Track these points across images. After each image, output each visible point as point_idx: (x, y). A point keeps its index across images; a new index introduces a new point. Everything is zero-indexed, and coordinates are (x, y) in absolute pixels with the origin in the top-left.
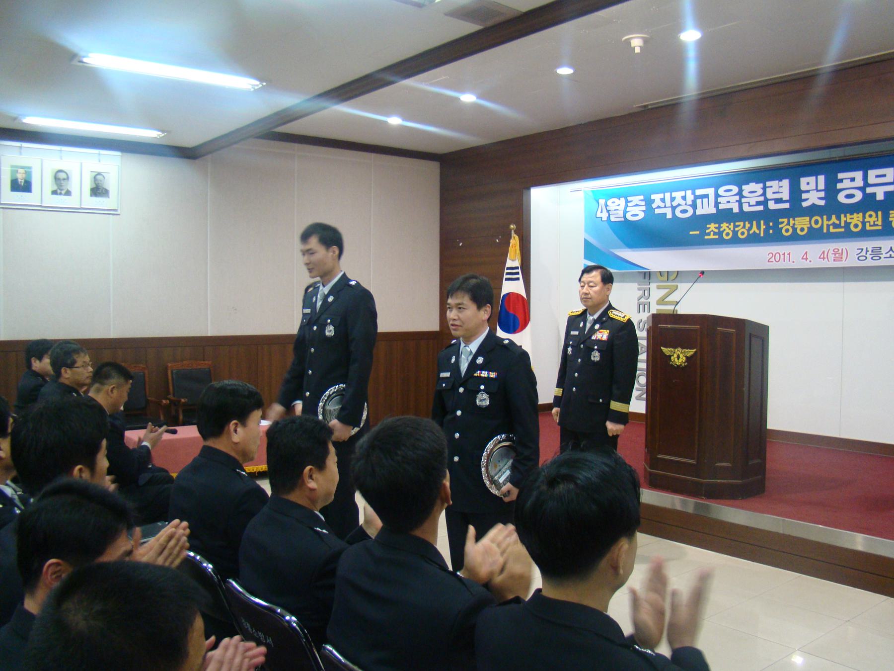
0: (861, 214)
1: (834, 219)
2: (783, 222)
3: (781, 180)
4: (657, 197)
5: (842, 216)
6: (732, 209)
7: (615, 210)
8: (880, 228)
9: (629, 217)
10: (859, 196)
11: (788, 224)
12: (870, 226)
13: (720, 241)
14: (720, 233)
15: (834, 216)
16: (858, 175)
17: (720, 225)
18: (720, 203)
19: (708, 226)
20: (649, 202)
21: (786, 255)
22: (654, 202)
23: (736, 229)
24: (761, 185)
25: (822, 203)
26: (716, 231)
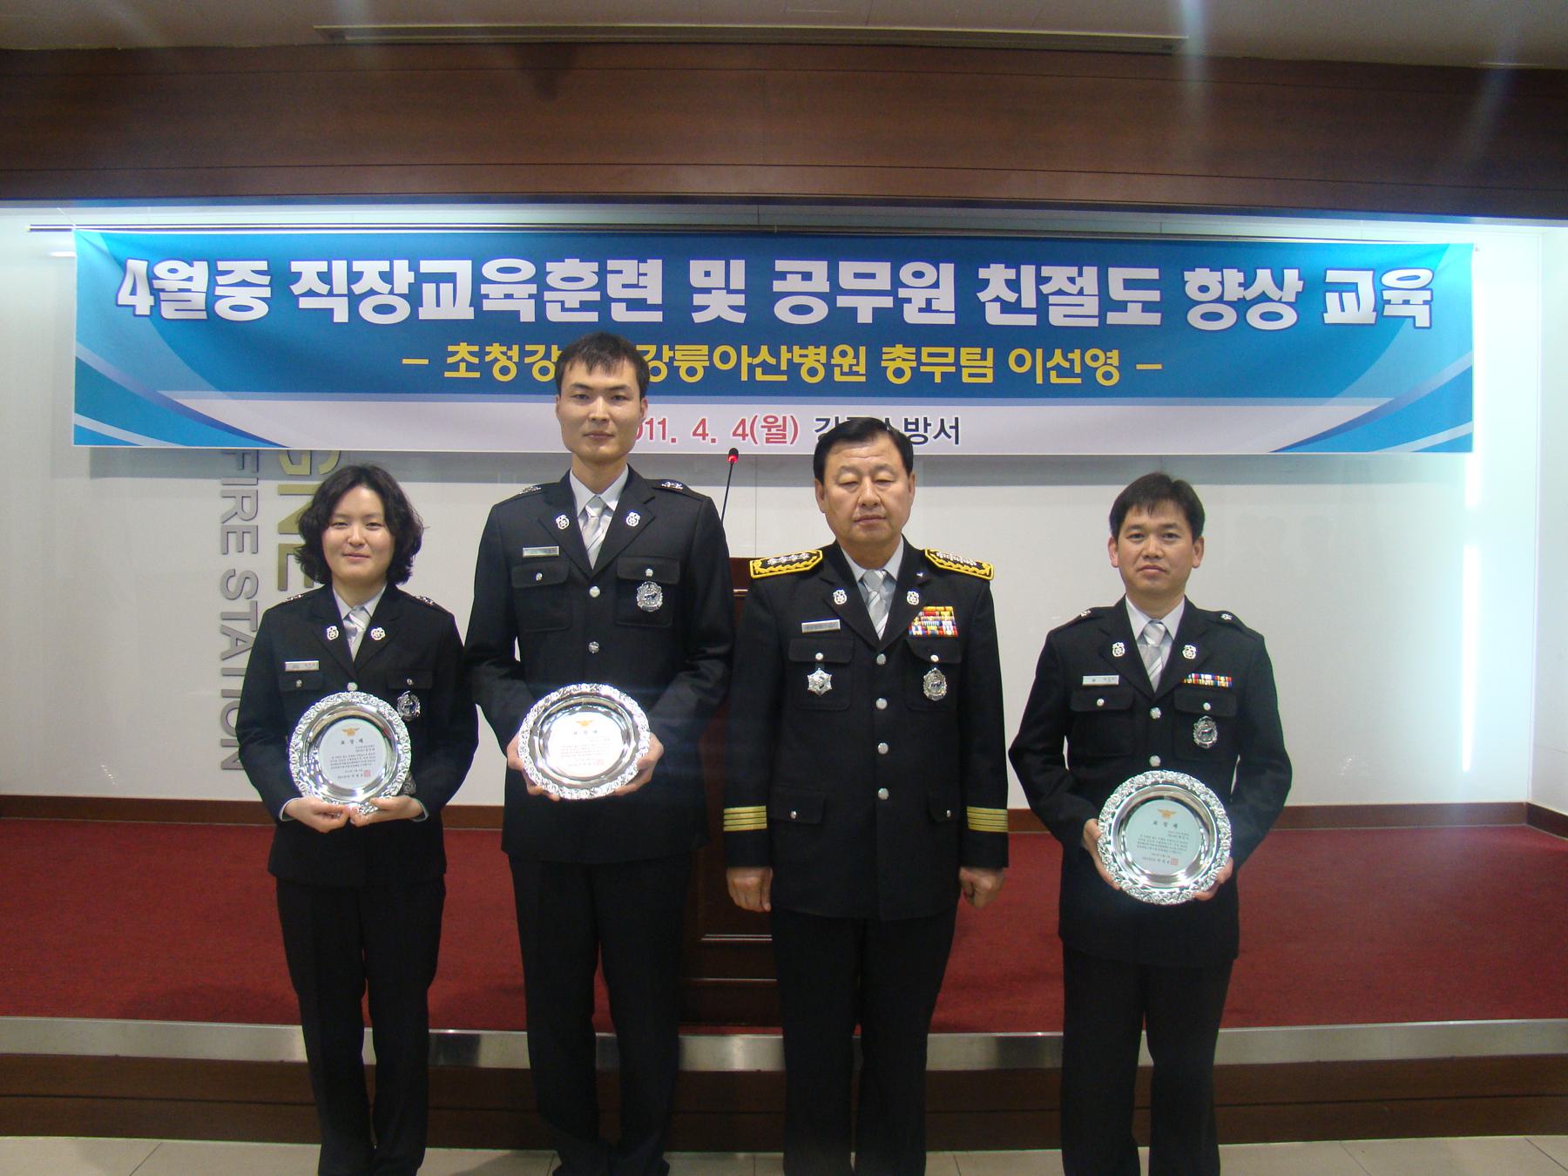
0: (823, 350)
1: (764, 354)
3: (642, 260)
4: (309, 270)
5: (784, 348)
6: (518, 313)
8: (863, 379)
9: (222, 308)
10: (820, 311)
11: (658, 356)
12: (843, 374)
13: (484, 385)
14: (485, 368)
15: (764, 349)
16: (819, 268)
18: (487, 296)
19: (451, 348)
20: (281, 279)
21: (655, 423)
23: (528, 360)
24: (595, 266)
25: (740, 318)
26: (476, 360)
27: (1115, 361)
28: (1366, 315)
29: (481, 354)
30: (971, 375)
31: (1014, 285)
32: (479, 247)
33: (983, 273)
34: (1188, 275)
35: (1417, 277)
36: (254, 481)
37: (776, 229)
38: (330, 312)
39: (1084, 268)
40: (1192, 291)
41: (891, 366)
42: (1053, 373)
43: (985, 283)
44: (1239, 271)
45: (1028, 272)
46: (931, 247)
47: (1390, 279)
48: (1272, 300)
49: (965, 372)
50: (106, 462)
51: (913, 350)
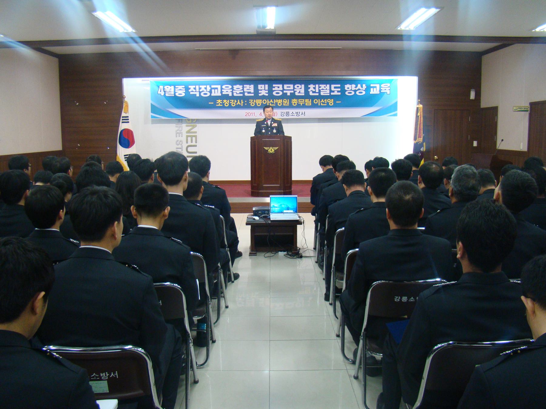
0: (281, 100)
1: (271, 101)
4: (192, 87)
5: (275, 100)
8: (288, 105)
9: (177, 94)
10: (281, 93)
11: (253, 102)
13: (223, 107)
14: (223, 104)
15: (271, 100)
16: (281, 86)
18: (223, 92)
19: (217, 101)
20: (187, 89)
23: (230, 103)
24: (242, 86)
25: (267, 95)
26: (222, 103)
29: (222, 102)
32: (222, 83)
33: (309, 86)
34: (345, 86)
35: (387, 85)
36: (181, 124)
40: (346, 89)
41: (293, 103)
42: (322, 103)
43: (309, 88)
44: (355, 85)
45: (317, 86)
46: (300, 82)
47: (382, 86)
49: (306, 103)
50: (155, 121)
51: (297, 100)
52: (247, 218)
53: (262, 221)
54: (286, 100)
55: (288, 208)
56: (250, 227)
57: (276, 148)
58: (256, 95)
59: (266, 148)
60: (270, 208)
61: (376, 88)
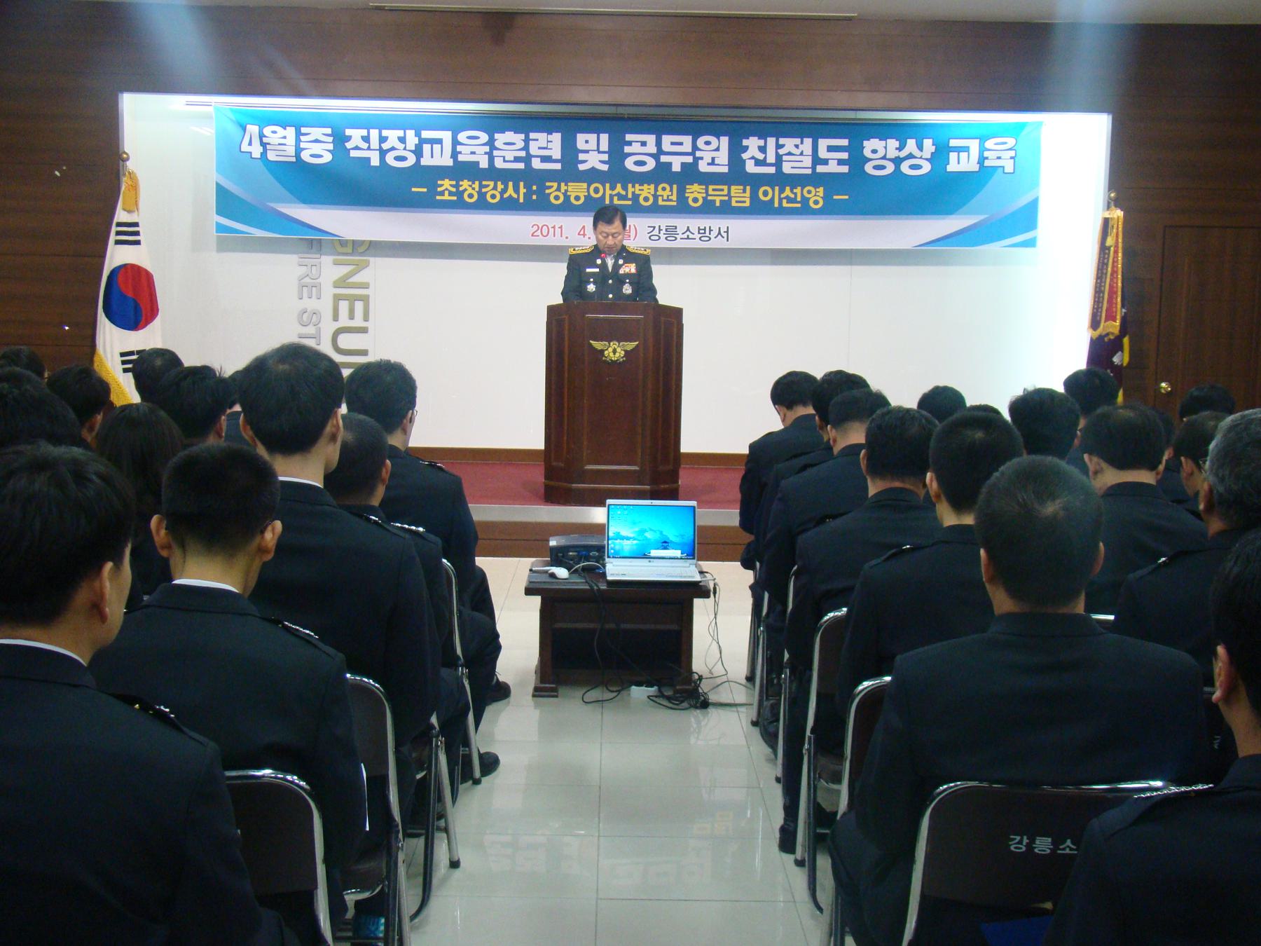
0: (652, 186)
1: (619, 188)
2: (552, 187)
3: (550, 133)
4: (356, 135)
5: (630, 185)
6: (478, 163)
7: (280, 144)
8: (675, 204)
9: (305, 156)
10: (651, 164)
11: (558, 189)
12: (663, 200)
13: (459, 204)
14: (460, 194)
15: (619, 186)
16: (651, 139)
17: (458, 183)
18: (460, 153)
19: (439, 182)
20: (340, 139)
21: (557, 227)
22: (350, 140)
23: (484, 190)
24: (522, 136)
25: (605, 168)
26: (454, 190)
27: (821, 194)
28: (973, 167)
29: (457, 186)
30: (737, 202)
31: (763, 149)
32: (456, 125)
33: (745, 142)
34: (866, 143)
35: (1006, 143)
36: (318, 256)
37: (626, 116)
38: (369, 159)
39: (805, 139)
40: (867, 153)
42: (784, 201)
45: (771, 142)
47: (989, 144)
48: (916, 158)
49: (734, 200)
50: (228, 242)
51: (704, 187)
52: (531, 570)
53: (580, 583)
54: (668, 188)
55: (665, 542)
56: (537, 600)
57: (631, 345)
58: (570, 169)
59: (597, 345)
60: (606, 542)
61: (968, 151)
